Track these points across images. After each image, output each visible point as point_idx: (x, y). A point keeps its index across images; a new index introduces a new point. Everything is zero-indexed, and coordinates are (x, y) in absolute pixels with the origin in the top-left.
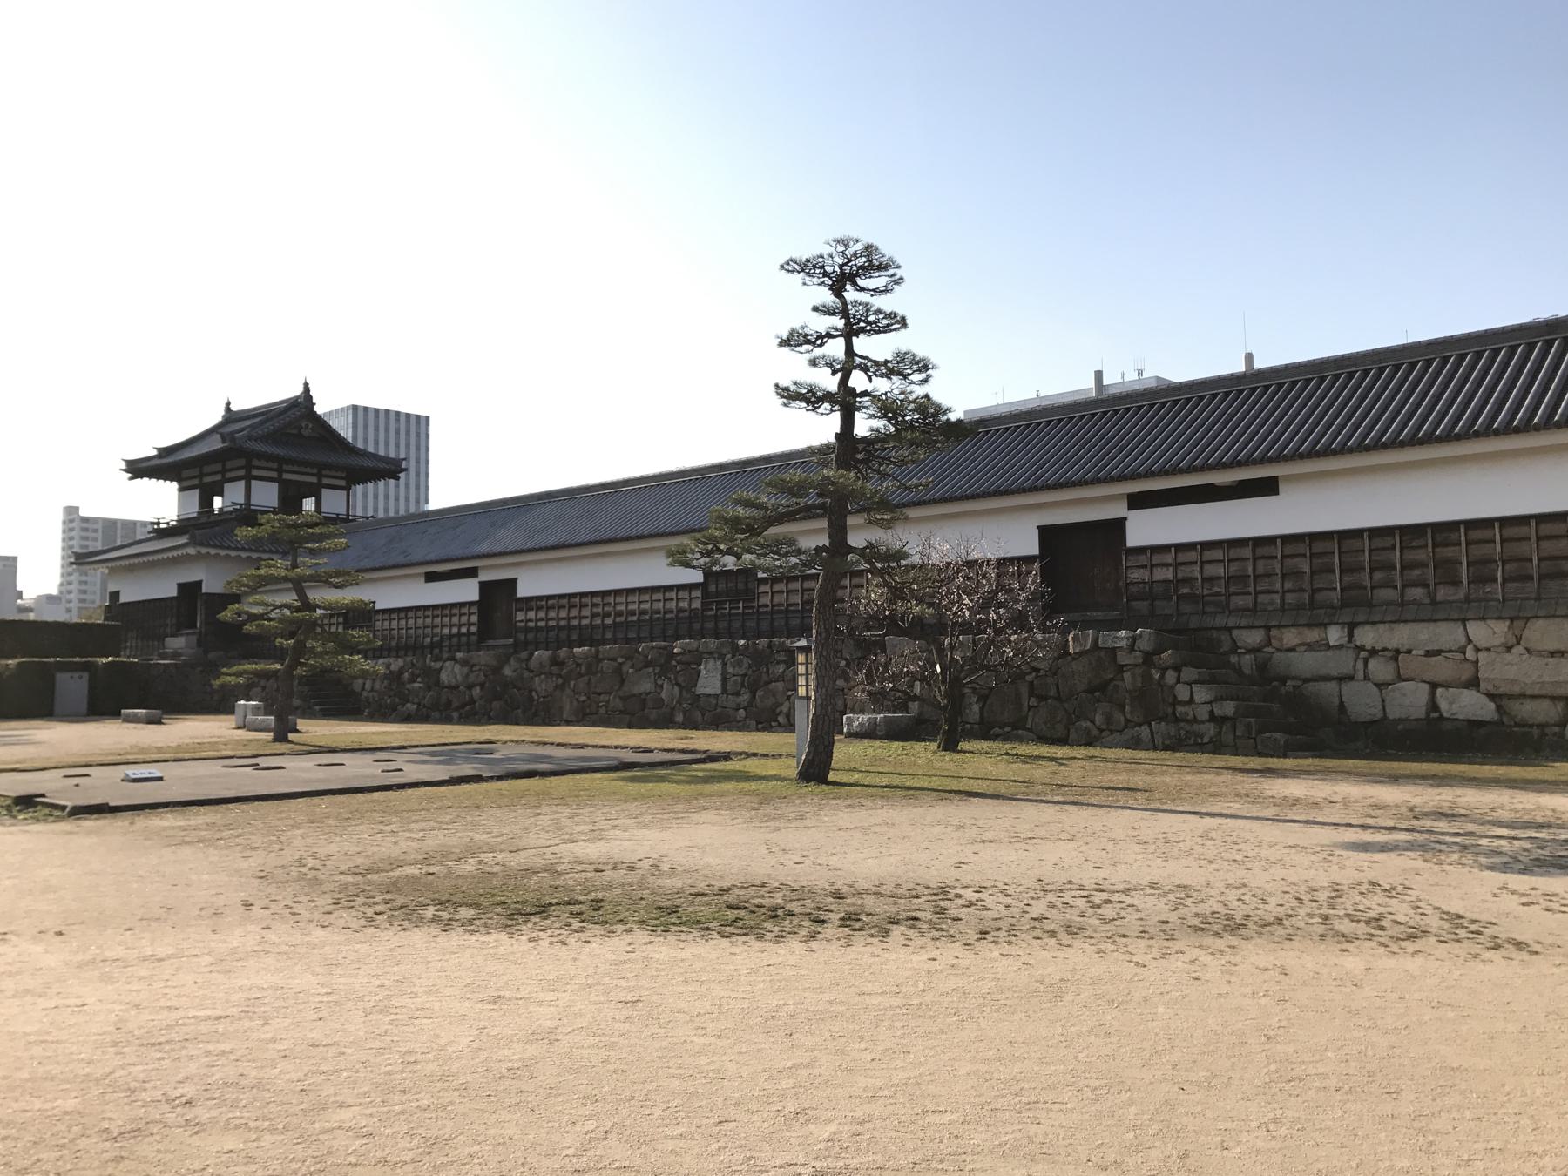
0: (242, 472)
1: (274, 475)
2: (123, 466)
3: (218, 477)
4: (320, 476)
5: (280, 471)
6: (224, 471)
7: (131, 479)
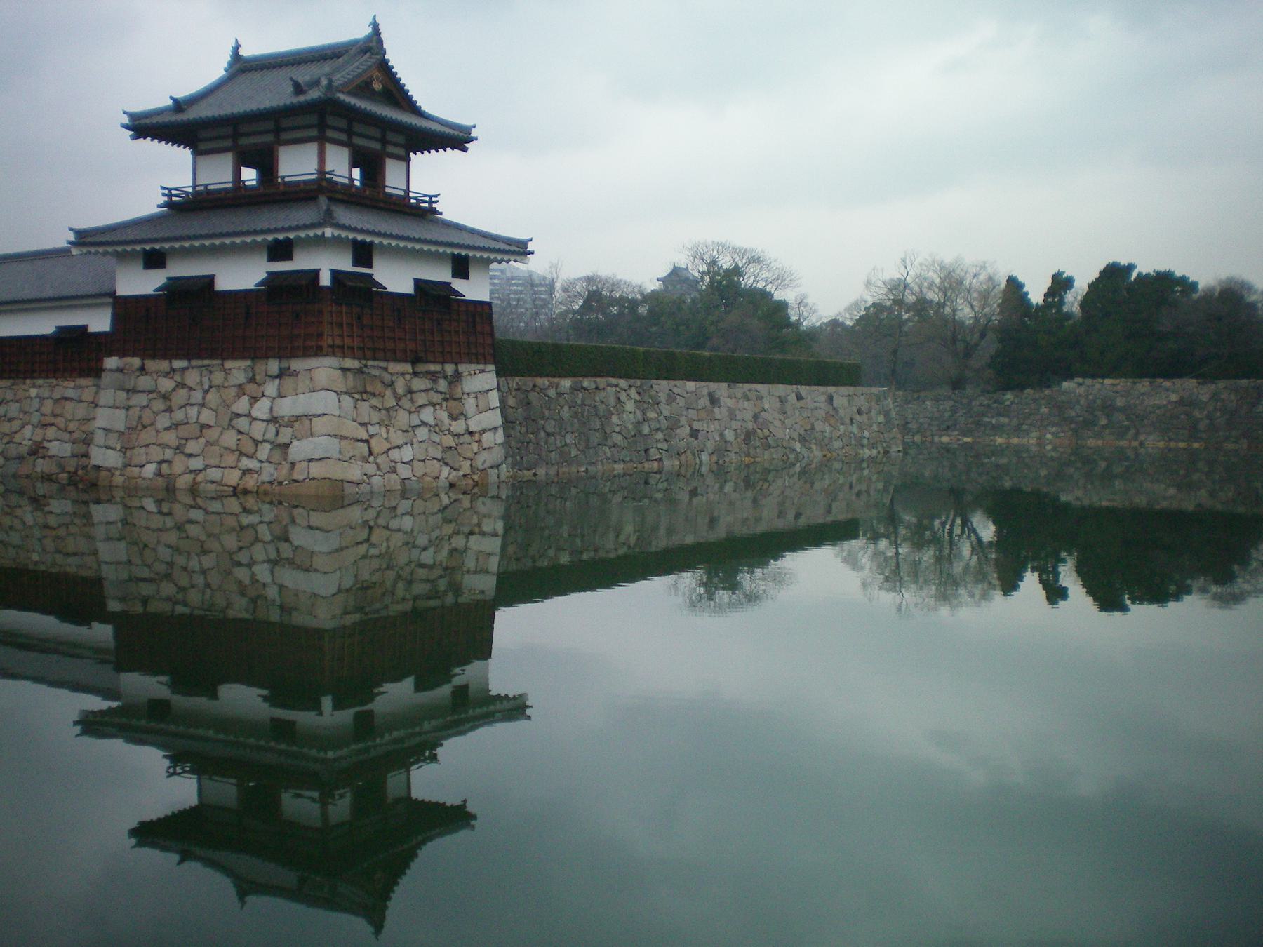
0: (314, 133)
1: (344, 137)
2: (126, 120)
3: (269, 138)
4: (384, 141)
5: (350, 132)
6: (277, 131)
7: (135, 138)
